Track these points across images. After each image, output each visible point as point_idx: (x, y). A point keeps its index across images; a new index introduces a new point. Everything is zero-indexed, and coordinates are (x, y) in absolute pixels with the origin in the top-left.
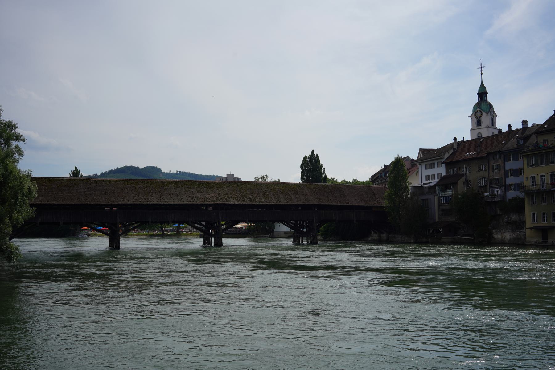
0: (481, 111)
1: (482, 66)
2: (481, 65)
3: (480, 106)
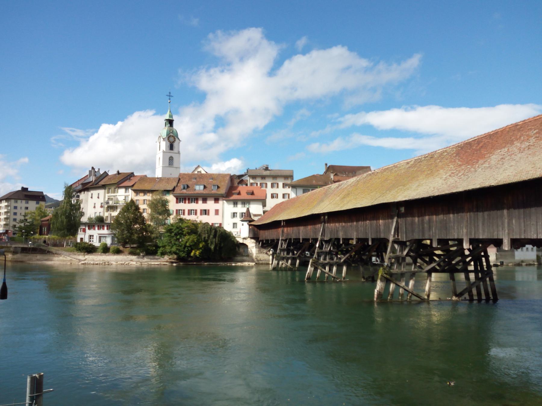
0: (174, 137)
1: (171, 95)
2: (170, 93)
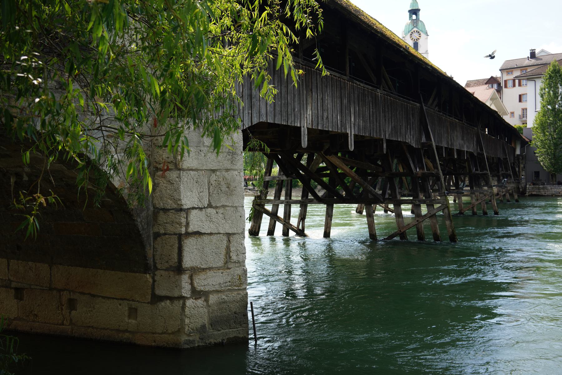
0: (419, 32)
3: (417, 25)
